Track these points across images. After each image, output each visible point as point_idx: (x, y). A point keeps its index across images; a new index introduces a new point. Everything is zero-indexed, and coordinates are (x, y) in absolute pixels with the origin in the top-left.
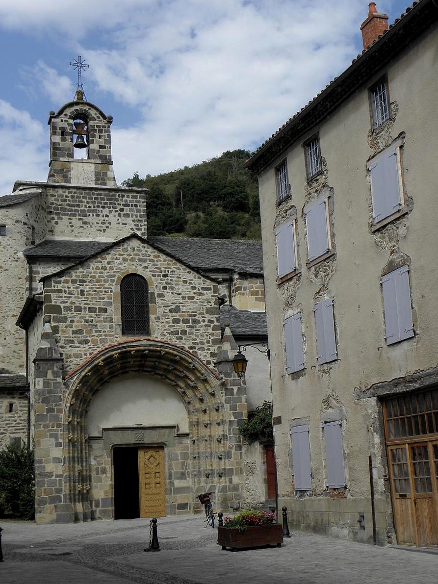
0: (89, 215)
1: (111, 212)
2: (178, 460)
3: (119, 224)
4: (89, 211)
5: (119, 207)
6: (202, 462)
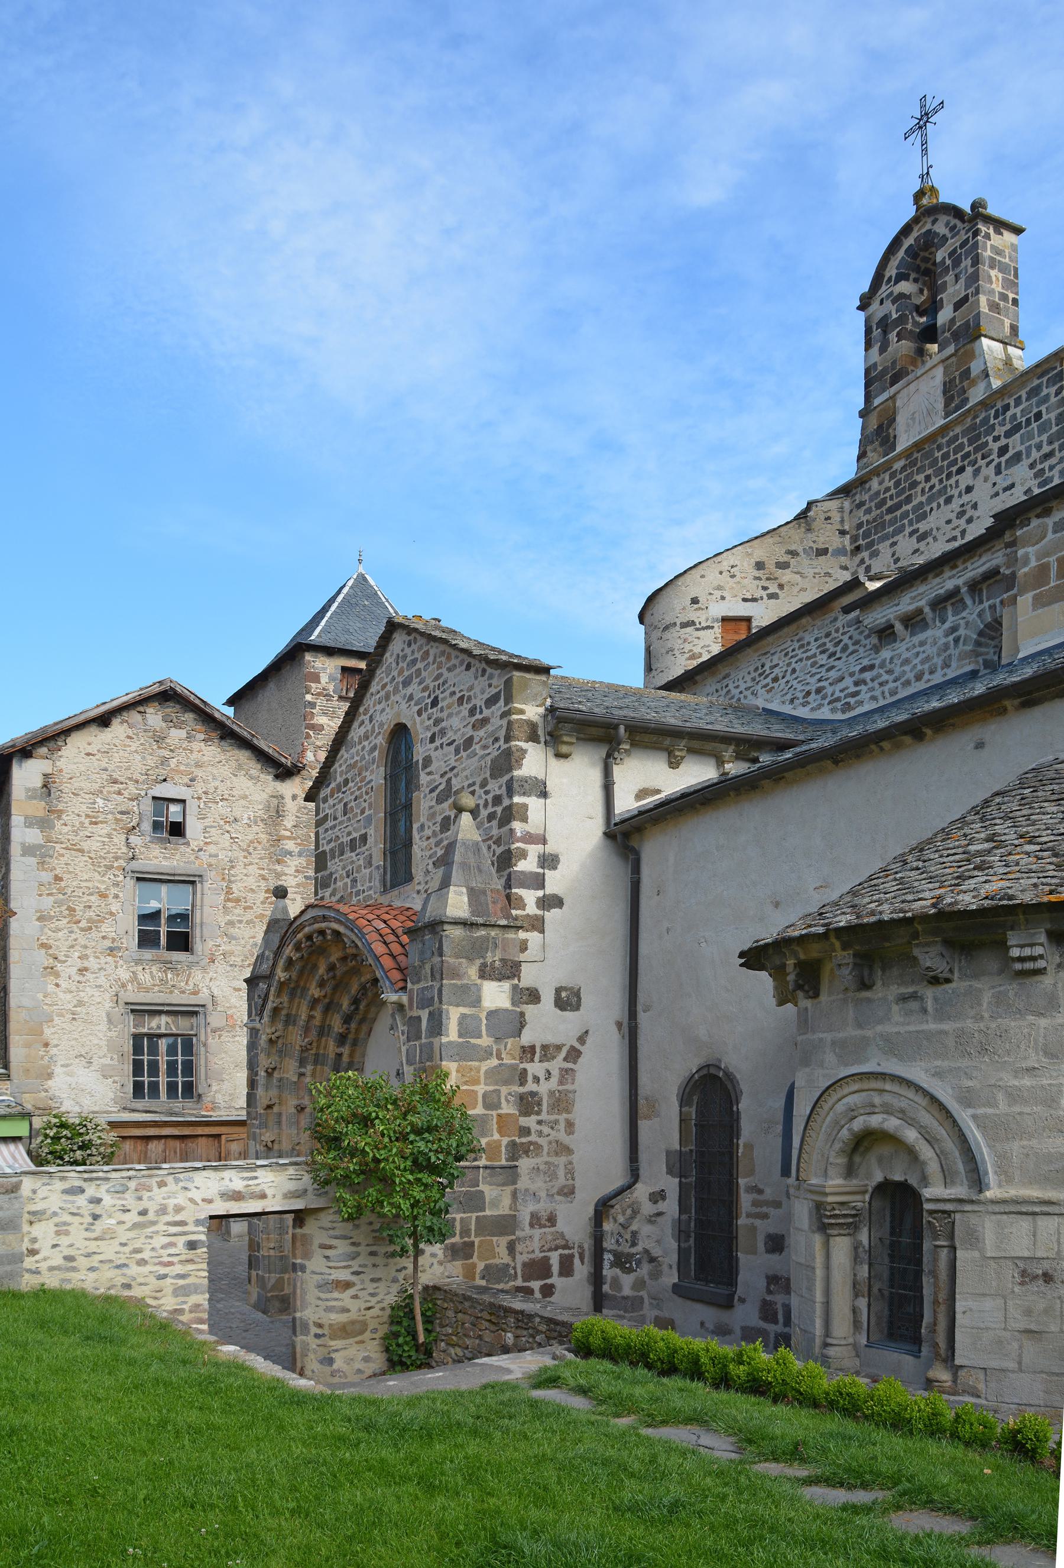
0: (932, 509)
1: (977, 472)
3: (997, 494)
4: (930, 500)
5: (995, 447)
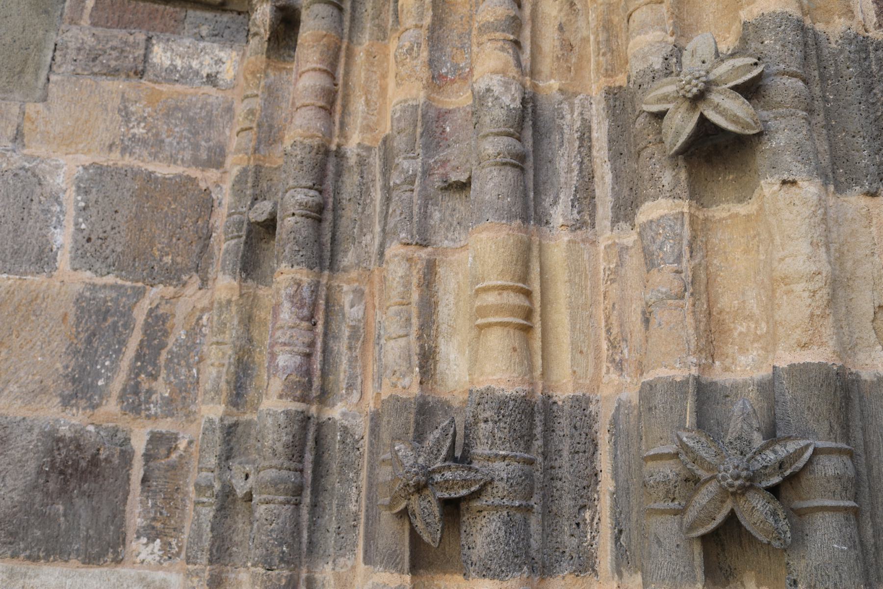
2: (44, 259)
6: (378, 280)
